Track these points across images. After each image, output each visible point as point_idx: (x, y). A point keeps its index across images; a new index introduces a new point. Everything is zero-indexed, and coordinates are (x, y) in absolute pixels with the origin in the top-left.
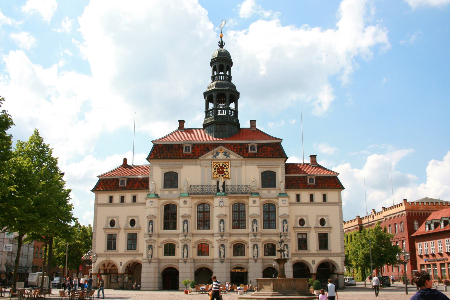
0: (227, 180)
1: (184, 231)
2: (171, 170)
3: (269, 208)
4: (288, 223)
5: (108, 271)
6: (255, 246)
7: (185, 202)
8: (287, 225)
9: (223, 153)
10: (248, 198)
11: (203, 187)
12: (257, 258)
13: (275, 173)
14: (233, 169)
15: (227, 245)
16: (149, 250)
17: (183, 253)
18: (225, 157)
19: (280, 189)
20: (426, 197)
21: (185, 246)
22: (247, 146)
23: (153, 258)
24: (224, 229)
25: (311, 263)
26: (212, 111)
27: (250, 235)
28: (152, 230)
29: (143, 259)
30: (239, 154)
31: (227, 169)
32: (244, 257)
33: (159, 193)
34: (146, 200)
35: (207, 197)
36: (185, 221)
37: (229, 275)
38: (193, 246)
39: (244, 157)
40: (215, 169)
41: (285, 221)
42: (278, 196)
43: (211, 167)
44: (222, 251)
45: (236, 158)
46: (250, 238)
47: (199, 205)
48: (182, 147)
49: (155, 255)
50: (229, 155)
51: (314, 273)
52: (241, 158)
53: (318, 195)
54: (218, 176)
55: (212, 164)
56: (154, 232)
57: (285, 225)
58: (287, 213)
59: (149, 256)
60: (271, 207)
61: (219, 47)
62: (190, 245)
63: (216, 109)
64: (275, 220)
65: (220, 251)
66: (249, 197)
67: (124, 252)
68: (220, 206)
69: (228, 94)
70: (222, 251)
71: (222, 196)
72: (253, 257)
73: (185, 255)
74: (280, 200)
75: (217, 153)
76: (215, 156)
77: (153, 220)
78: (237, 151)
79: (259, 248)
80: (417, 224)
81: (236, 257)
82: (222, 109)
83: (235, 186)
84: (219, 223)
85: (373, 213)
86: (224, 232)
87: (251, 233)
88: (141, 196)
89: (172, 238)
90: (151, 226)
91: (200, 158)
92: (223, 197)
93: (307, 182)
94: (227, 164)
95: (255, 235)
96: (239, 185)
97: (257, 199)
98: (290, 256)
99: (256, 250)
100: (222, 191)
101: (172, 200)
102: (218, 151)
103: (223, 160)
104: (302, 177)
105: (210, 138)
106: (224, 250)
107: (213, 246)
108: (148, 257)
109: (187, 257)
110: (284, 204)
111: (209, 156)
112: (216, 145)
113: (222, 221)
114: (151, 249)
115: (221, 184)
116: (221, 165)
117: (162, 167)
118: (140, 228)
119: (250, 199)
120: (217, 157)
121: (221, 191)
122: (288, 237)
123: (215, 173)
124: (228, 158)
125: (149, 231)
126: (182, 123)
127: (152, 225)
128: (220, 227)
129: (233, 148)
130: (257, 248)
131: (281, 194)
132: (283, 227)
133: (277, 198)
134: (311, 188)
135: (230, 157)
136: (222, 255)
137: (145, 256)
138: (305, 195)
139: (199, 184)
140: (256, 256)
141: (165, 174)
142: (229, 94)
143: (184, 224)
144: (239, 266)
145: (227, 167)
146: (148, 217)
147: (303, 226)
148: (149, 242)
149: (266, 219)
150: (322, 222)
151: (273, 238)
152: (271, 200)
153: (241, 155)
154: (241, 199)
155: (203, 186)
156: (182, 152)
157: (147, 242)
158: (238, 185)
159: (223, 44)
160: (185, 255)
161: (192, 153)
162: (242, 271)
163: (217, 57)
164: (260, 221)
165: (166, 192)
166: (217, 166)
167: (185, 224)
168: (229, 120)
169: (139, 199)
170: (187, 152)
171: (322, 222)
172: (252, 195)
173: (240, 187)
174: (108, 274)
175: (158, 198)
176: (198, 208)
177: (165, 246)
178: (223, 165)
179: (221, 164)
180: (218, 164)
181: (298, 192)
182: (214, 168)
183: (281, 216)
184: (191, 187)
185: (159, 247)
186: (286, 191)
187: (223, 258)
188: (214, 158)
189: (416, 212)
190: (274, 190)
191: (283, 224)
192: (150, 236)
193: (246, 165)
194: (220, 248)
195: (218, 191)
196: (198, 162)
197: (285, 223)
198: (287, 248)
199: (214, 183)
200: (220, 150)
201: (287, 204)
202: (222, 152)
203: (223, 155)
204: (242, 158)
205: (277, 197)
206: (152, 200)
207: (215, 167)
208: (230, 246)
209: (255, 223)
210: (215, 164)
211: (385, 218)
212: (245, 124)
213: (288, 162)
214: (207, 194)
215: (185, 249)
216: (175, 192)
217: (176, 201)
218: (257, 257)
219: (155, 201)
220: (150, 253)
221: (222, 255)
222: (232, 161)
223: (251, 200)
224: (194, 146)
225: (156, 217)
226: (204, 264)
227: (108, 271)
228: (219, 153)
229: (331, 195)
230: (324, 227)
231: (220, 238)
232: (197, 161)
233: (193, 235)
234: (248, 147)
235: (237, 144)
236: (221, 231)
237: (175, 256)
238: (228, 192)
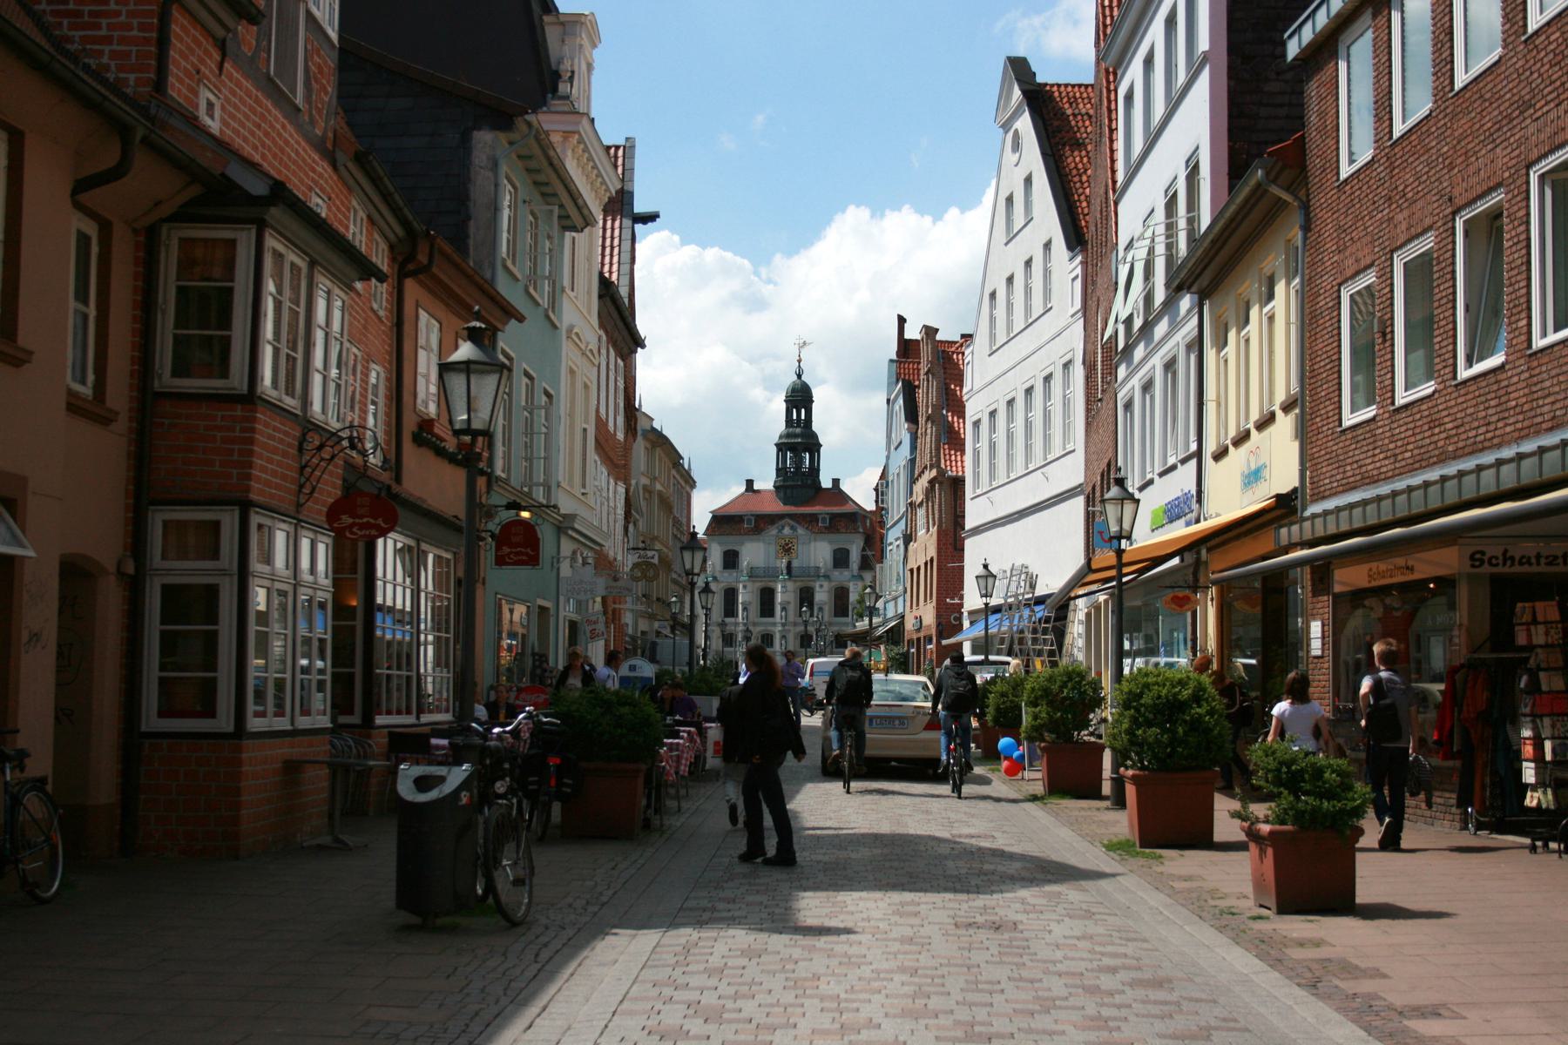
2: (730, 548)
7: (745, 587)
15: (791, 637)
33: (717, 574)
61: (795, 378)
75: (783, 528)
76: (780, 531)
97: (826, 584)
112: (781, 517)
126: (750, 483)
139: (762, 565)
165: (726, 575)
193: (815, 540)
212: (826, 483)
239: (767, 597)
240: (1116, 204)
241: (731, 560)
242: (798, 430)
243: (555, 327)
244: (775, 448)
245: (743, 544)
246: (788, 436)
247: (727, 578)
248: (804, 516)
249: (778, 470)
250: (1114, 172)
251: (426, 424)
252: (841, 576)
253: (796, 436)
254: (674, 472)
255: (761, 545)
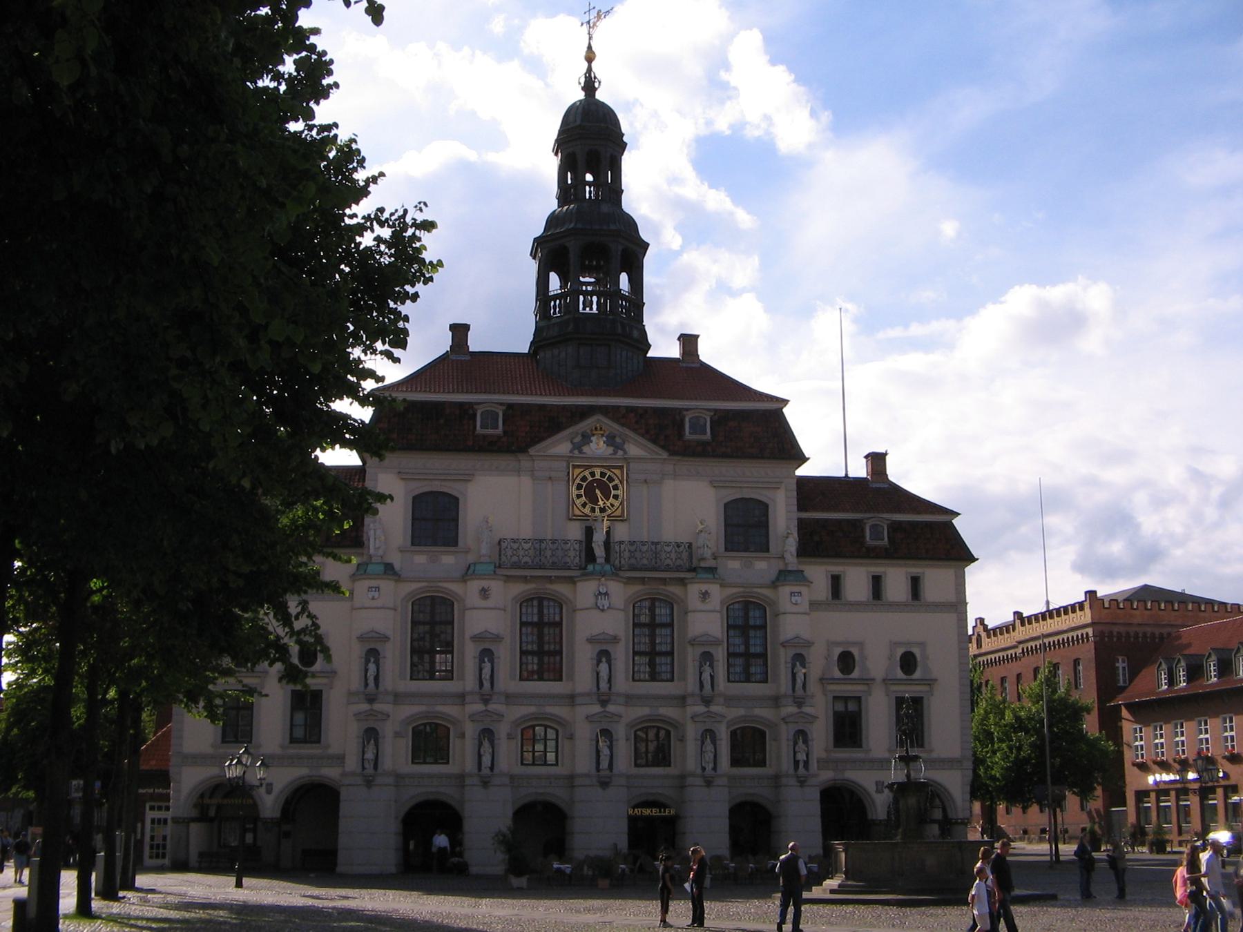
0: (615, 522)
1: (481, 685)
2: (436, 486)
3: (746, 617)
4: (807, 665)
5: (212, 813)
6: (709, 735)
7: (484, 593)
8: (804, 671)
9: (604, 439)
10: (682, 582)
11: (543, 546)
12: (713, 772)
13: (766, 506)
15: (621, 732)
16: (368, 743)
17: (480, 756)
18: (611, 450)
19: (783, 558)
20: (1146, 585)
21: (487, 734)
22: (678, 417)
23: (380, 770)
24: (609, 681)
25: (871, 788)
26: (558, 302)
27: (689, 701)
28: (377, 678)
29: (344, 774)
30: (654, 441)
31: (616, 487)
32: (668, 769)
33: (396, 560)
34: (354, 581)
35: (557, 577)
37: (624, 826)
38: (508, 735)
39: (673, 453)
40: (579, 487)
41: (800, 659)
42: (778, 579)
43: (565, 483)
44: (605, 751)
45: (647, 454)
46: (690, 710)
47: (525, 601)
48: (471, 412)
49: (387, 763)
50: (624, 443)
51: (880, 820)
52: (660, 455)
53: (896, 579)
54: (587, 510)
55: (569, 473)
56: (381, 688)
57: (801, 672)
58: (806, 634)
59: (366, 765)
60: (751, 614)
61: (581, 95)
62: (502, 730)
63: (572, 292)
64: (764, 656)
65: (598, 752)
66: (687, 581)
67: (278, 751)
68: (599, 608)
70: (605, 751)
72: (699, 771)
73: (486, 760)
74: (785, 590)
75: (586, 439)
76: (578, 447)
77: (378, 646)
78: (647, 432)
79: (718, 742)
80: (1124, 668)
81: (643, 771)
82: (592, 294)
83: (643, 544)
84: (595, 662)
85: (980, 628)
86: (610, 688)
87: (693, 695)
89: (440, 708)
90: (372, 667)
91: (532, 451)
92: (606, 580)
93: (863, 537)
94: (617, 472)
95: (707, 701)
96: (658, 543)
97: (714, 589)
98: (814, 765)
99: (709, 747)
100: (603, 560)
101: (440, 584)
102: (588, 431)
103: (606, 459)
104: (848, 521)
106: (611, 748)
107: (572, 735)
108: (364, 768)
109: (492, 768)
110: (796, 604)
111: (560, 446)
113: (604, 656)
114: (372, 742)
116: (598, 476)
119: (689, 586)
120: (585, 449)
121: (599, 561)
122: (807, 709)
123: (578, 502)
124: (620, 453)
125: (366, 685)
126: (460, 331)
127: (377, 663)
128: (598, 674)
129: (637, 422)
130: (714, 742)
131: (784, 576)
132: (794, 676)
133: (774, 585)
134: (878, 557)
135: (625, 452)
136: (604, 764)
137: (352, 763)
138: (856, 579)
139: (526, 532)
140: (711, 765)
141: (415, 498)
142: (620, 248)
143: (482, 661)
144: (651, 798)
145: (617, 482)
146: (362, 639)
147: (911, 674)
148: (367, 720)
149: (643, 648)
150: (908, 662)
151: (757, 711)
152: (755, 590)
153: (663, 447)
154: (663, 587)
155: (541, 541)
156: (471, 428)
157: (358, 720)
158: (653, 543)
159: (596, 85)
160: (486, 760)
161: (505, 432)
162: (660, 812)
163: (580, 125)
164: (720, 654)
165: (421, 559)
166: (584, 479)
167: (484, 662)
168: (620, 331)
170: (490, 431)
171: (908, 662)
172: (699, 576)
173: (659, 547)
174: (211, 820)
175: (396, 578)
176: (524, 610)
177: (417, 733)
178: (603, 475)
179: (598, 472)
180: (587, 473)
181: (836, 569)
182: (575, 484)
183: (787, 642)
184: (504, 545)
185: (397, 735)
186: (799, 563)
187: (607, 772)
188: (576, 452)
189: (1122, 629)
190: (763, 559)
191: (794, 666)
192: (371, 699)
193: (675, 476)
194: (598, 741)
195: (590, 556)
196: (525, 463)
197: (798, 663)
198: (803, 743)
199: (575, 532)
200: (596, 429)
201: (805, 606)
202: (603, 435)
203: (604, 442)
204: (665, 455)
205: (773, 582)
206: (374, 583)
207: (578, 481)
208: (626, 736)
209: (708, 663)
210: (577, 471)
211: (1021, 646)
213: (802, 471)
214: (554, 566)
215: (486, 744)
216: (449, 560)
217: (455, 587)
218: (715, 769)
219: (387, 585)
220: (370, 755)
221: (604, 764)
222: (632, 465)
223: (694, 590)
224: (511, 411)
225: (389, 639)
226: (541, 791)
227: (212, 813)
228: (592, 438)
229: (935, 578)
230: (851, 679)
231: (597, 709)
232: (519, 460)
234: (682, 421)
235: (646, 410)
236: (601, 686)
237: (448, 763)
238: (623, 562)
248: (642, 413)
255: (526, 481)
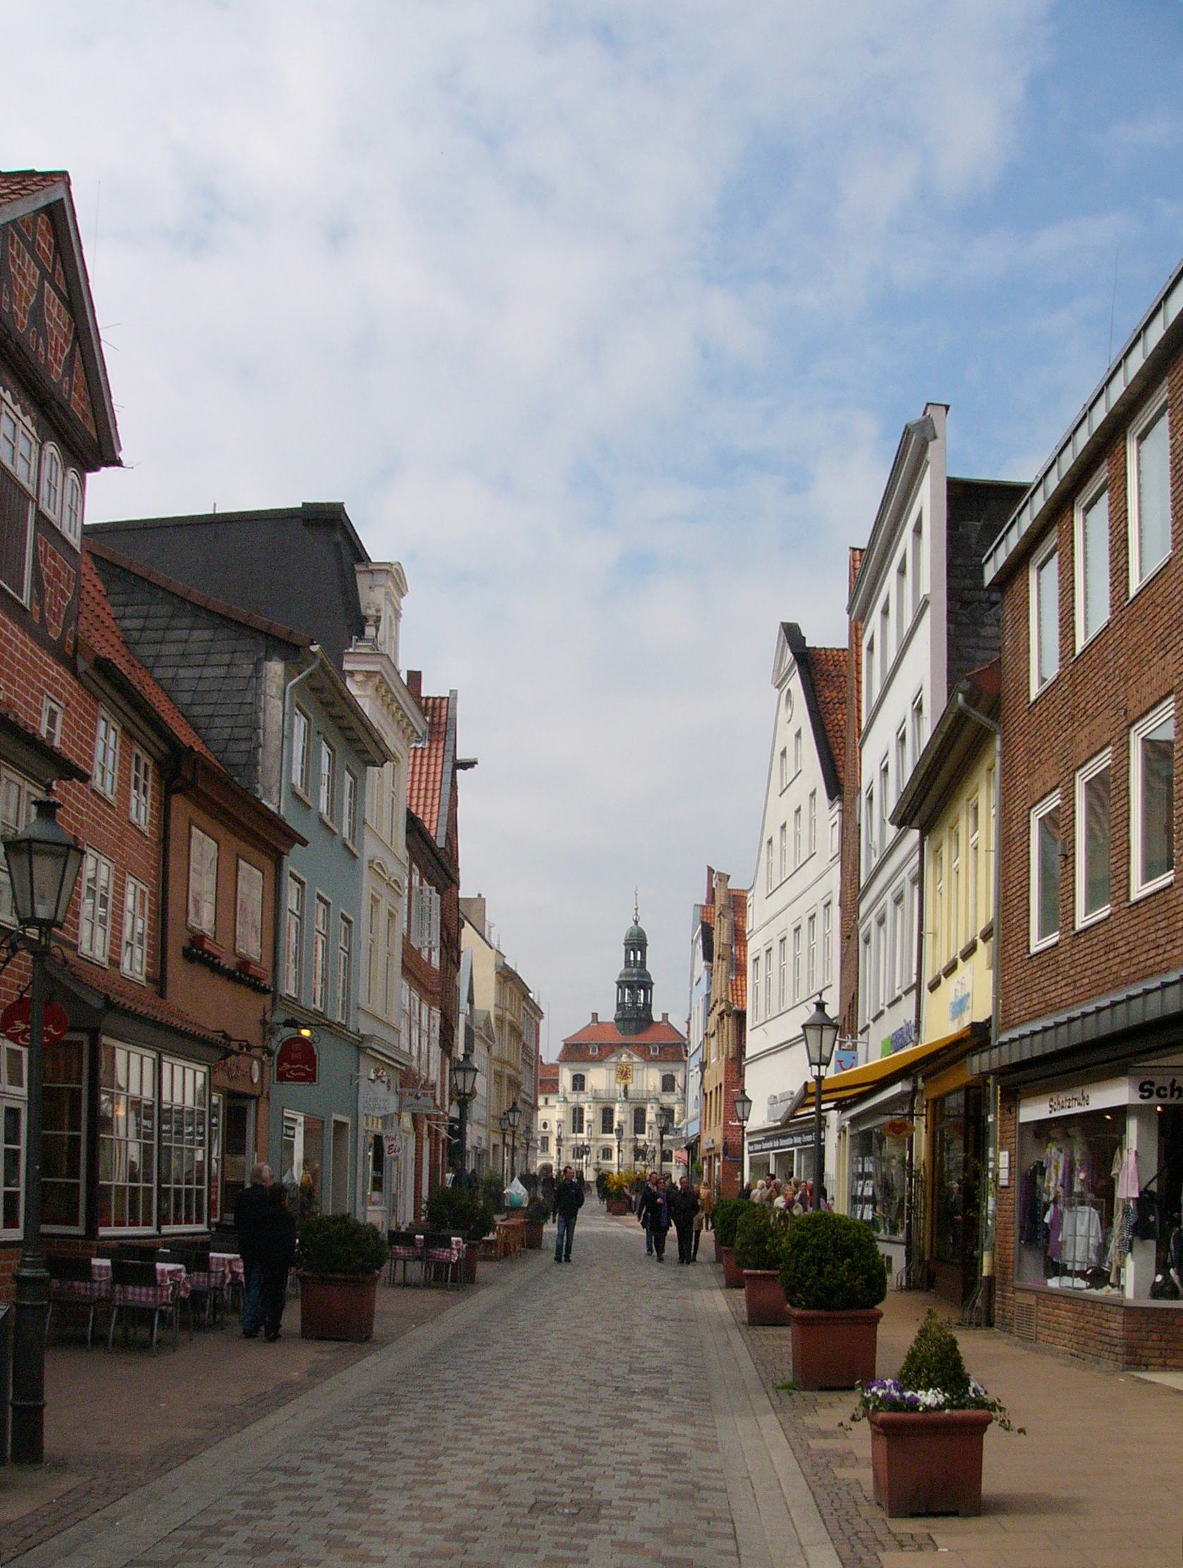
7: (590, 1107)
14: (635, 1073)
30: (641, 1056)
36: (589, 1126)
69: (635, 985)
71: (622, 1102)
88: (552, 1101)
105: (617, 1038)
112: (622, 1045)
115: (622, 1089)
117: (570, 1070)
118: (551, 1132)
126: (595, 1015)
137: (555, 1160)
165: (575, 1096)
169: (551, 1102)
212: (657, 1017)
233: (598, 1140)
239: (608, 1114)
240: (860, 749)
241: (579, 1083)
242: (635, 971)
243: (355, 856)
244: (616, 986)
245: (588, 1070)
246: (626, 975)
247: (573, 1098)
249: (618, 1005)
250: (860, 720)
251: (198, 939)
252: (669, 1099)
253: (633, 975)
254: (524, 1004)
